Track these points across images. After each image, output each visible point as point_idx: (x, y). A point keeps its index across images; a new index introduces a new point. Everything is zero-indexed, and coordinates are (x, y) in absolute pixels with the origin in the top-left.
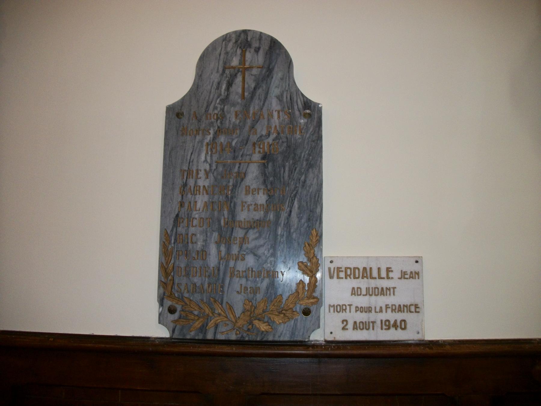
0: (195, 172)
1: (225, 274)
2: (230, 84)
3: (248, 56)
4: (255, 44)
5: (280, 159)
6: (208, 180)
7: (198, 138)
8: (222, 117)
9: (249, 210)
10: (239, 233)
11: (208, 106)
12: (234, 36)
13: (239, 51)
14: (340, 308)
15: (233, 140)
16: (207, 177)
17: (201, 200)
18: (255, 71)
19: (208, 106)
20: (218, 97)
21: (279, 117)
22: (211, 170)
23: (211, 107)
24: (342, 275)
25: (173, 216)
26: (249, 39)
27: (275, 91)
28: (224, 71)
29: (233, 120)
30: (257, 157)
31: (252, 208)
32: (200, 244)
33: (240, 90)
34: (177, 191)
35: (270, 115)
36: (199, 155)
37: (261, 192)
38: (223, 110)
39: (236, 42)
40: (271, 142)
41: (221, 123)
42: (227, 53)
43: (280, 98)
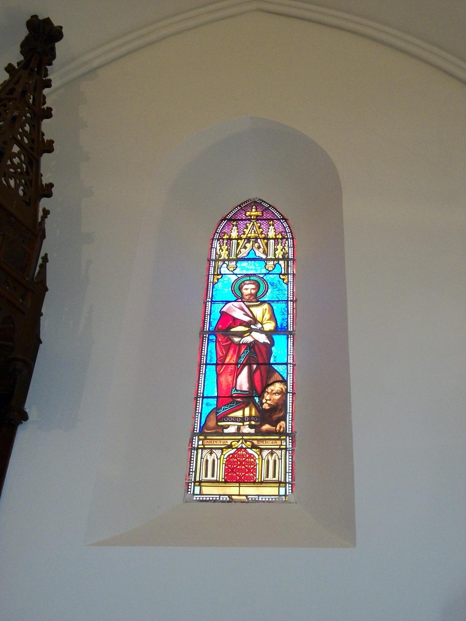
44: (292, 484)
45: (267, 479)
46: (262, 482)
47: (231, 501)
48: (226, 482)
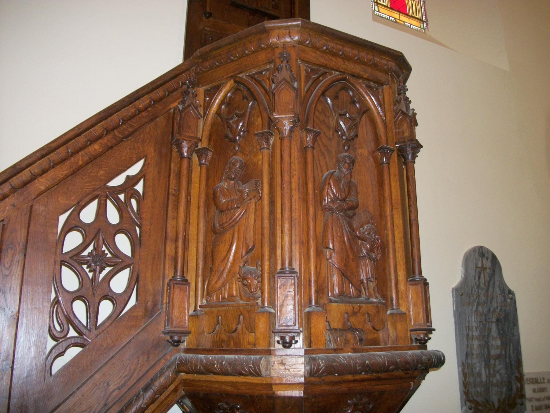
0: (471, 328)
1: (489, 384)
2: (479, 278)
3: (484, 261)
4: (486, 256)
5: (503, 321)
6: (477, 332)
7: (471, 307)
8: (478, 296)
9: (495, 349)
10: (492, 362)
11: (472, 290)
12: (477, 249)
13: (480, 259)
14: (531, 400)
15: (484, 310)
16: (476, 331)
17: (476, 343)
18: (488, 271)
19: (472, 290)
20: (475, 285)
21: (500, 298)
22: (477, 326)
23: (473, 290)
24: (529, 382)
25: (465, 353)
26: (483, 252)
27: (497, 283)
28: (476, 270)
29: (483, 298)
30: (494, 319)
31: (496, 347)
32: (478, 368)
33: (484, 282)
34: (465, 339)
35: (497, 296)
36: (472, 317)
37: (498, 339)
38: (478, 292)
39: (479, 252)
40: (499, 311)
41: (479, 299)
42: (476, 259)
43: (499, 287)
44: (426, 23)
45: (413, 15)
46: (412, 17)
47: (396, 22)
48: (392, 8)
